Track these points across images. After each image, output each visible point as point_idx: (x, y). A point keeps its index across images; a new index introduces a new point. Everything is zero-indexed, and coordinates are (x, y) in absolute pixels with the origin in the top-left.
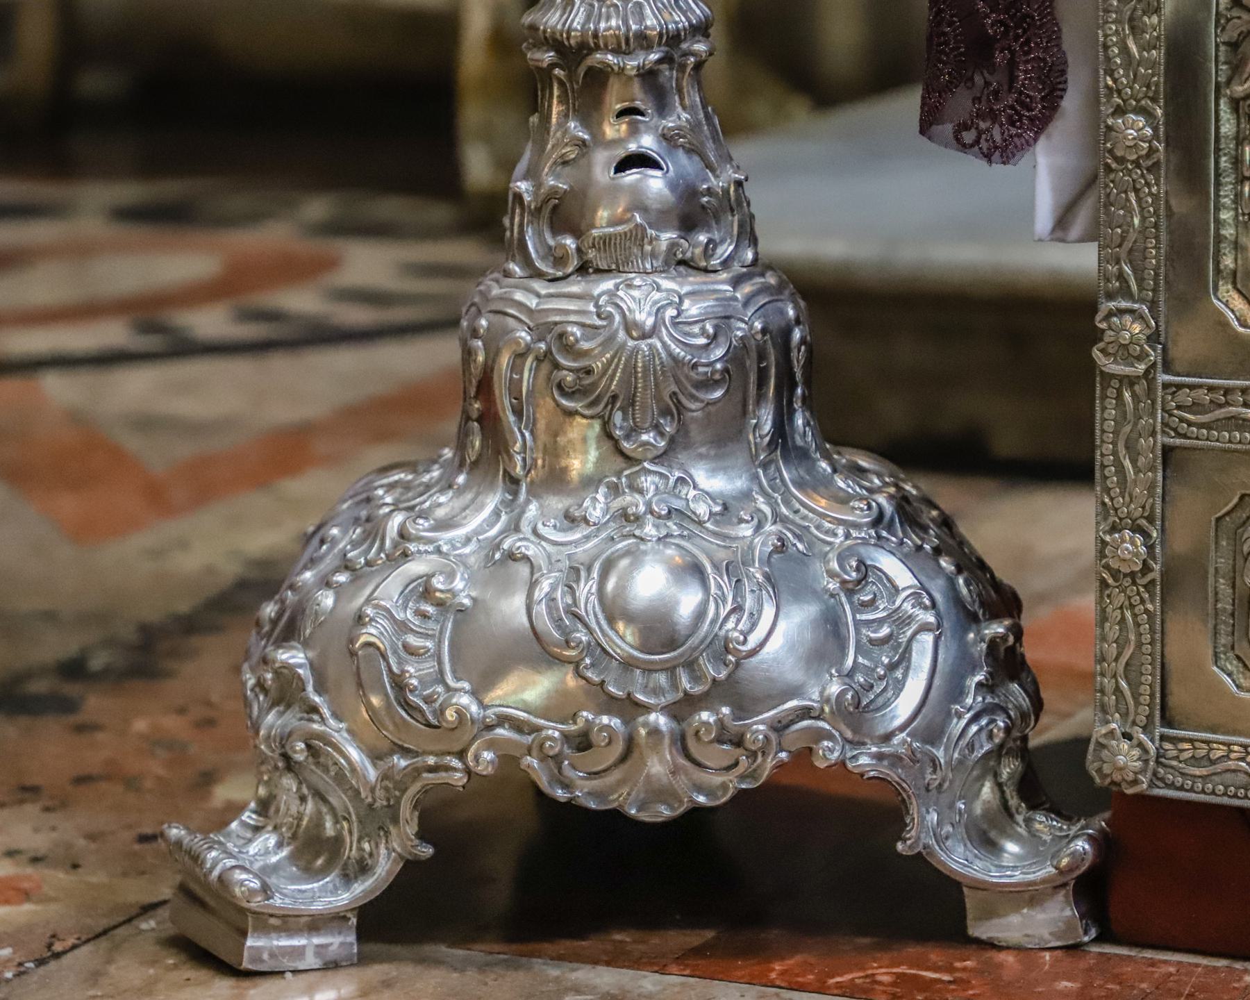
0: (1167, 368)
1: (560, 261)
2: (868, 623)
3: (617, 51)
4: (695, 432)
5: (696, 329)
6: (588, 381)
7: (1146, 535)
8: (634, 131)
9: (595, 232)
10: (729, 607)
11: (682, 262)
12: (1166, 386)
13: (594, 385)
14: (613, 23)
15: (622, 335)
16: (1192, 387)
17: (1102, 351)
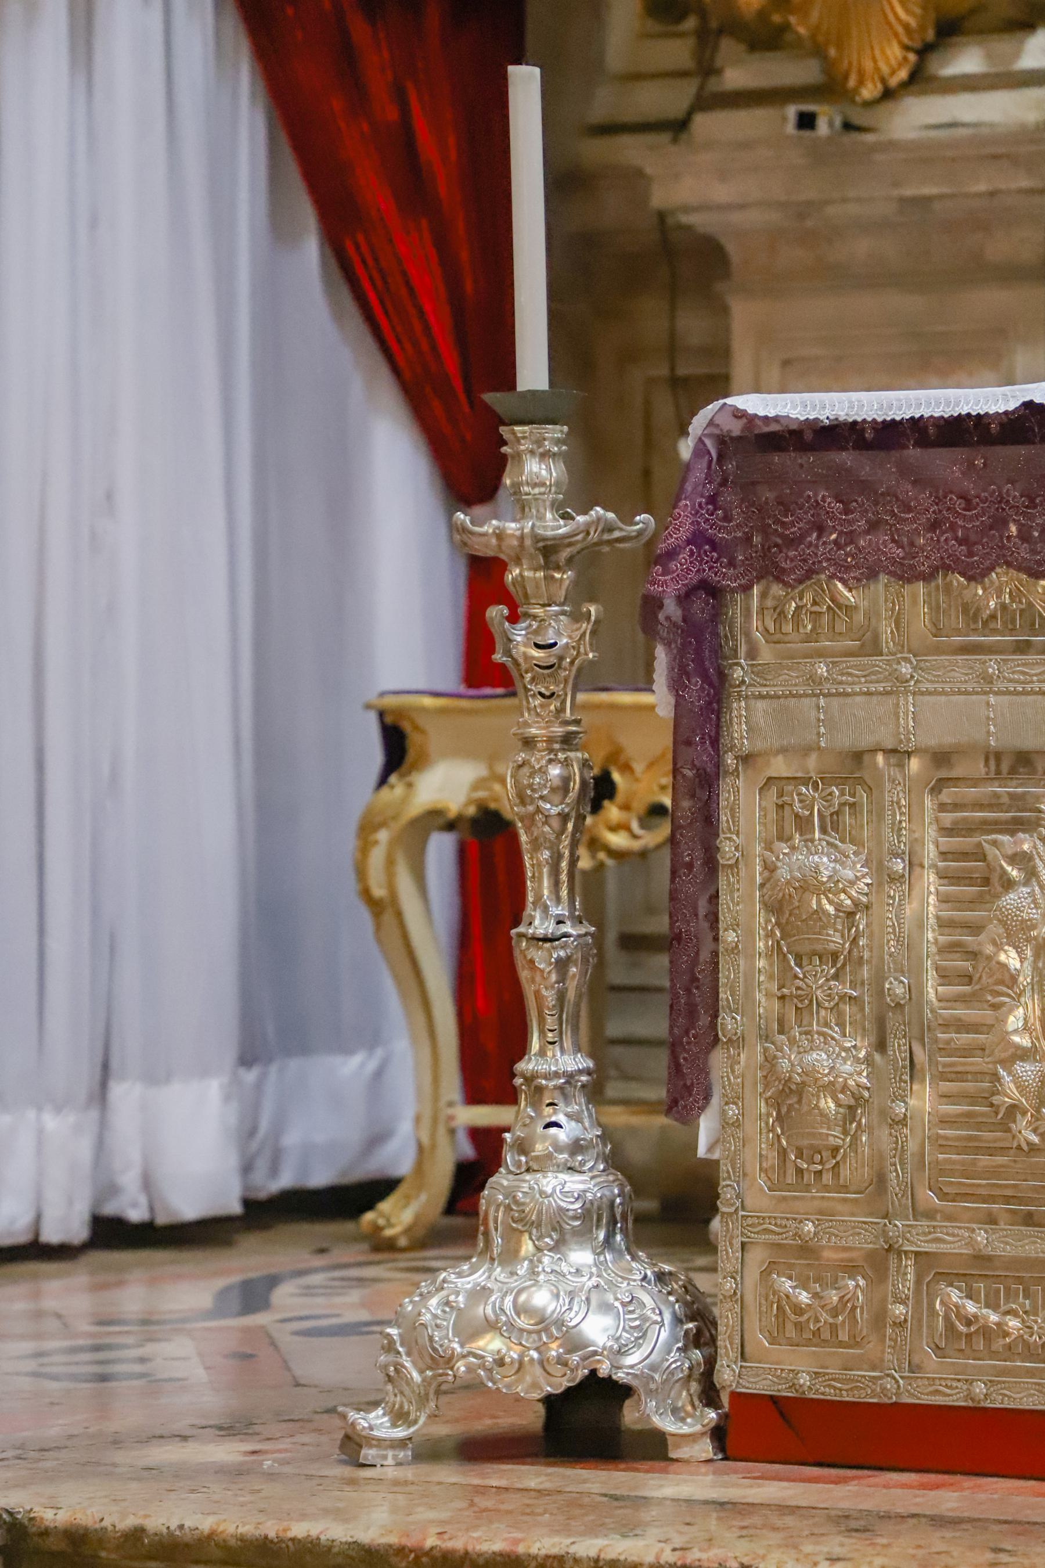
0: (743, 1208)
1: (519, 1166)
2: (630, 1319)
3: (546, 1078)
4: (568, 1237)
5: (569, 1194)
6: (523, 1215)
7: (735, 1279)
8: (555, 1112)
9: (533, 1154)
10: (567, 1307)
11: (570, 1168)
12: (743, 1216)
13: (526, 1217)
14: (544, 1067)
15: (538, 1196)
16: (751, 1217)
17: (721, 1202)
